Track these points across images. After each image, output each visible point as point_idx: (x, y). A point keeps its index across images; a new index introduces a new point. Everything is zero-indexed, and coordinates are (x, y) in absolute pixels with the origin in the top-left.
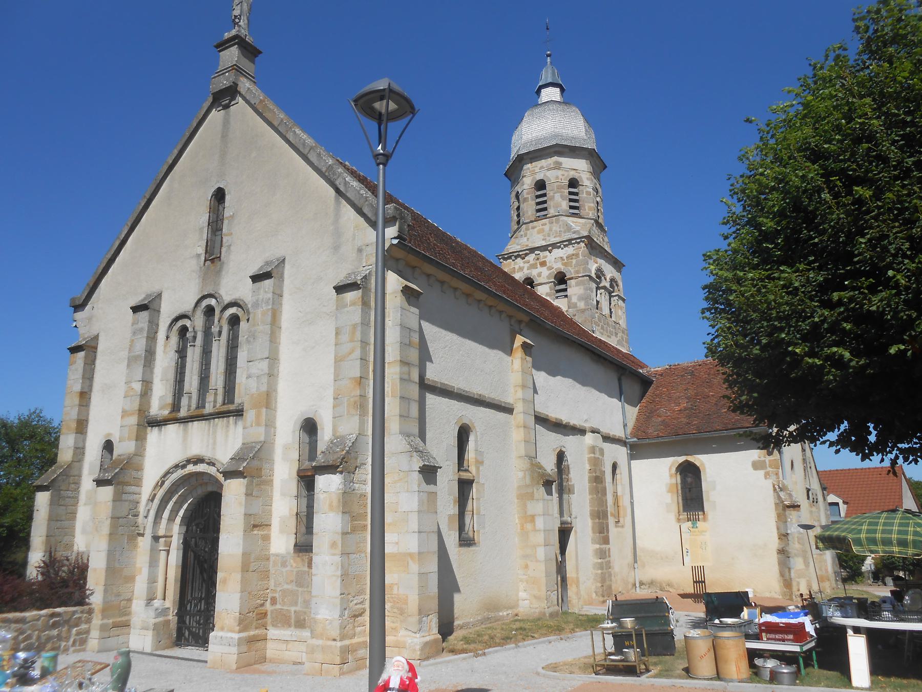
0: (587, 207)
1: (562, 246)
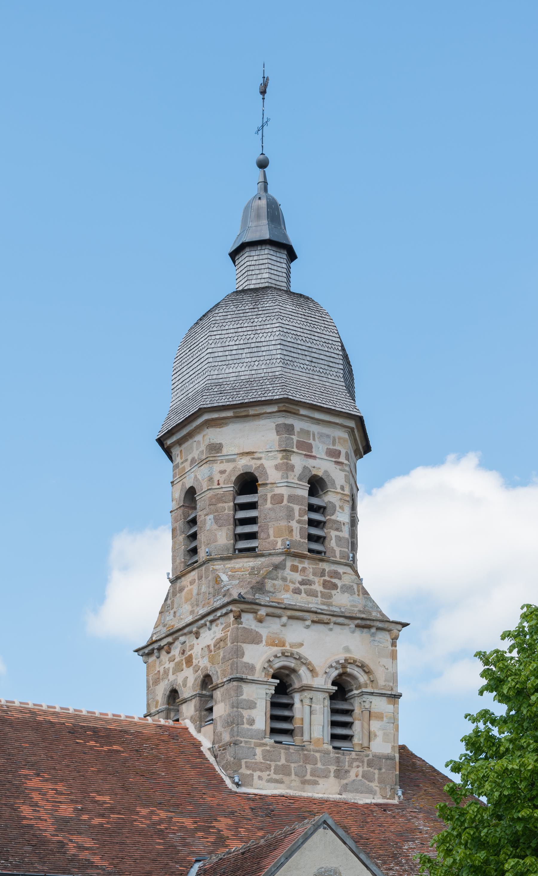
0: (271, 532)
1: (208, 623)
